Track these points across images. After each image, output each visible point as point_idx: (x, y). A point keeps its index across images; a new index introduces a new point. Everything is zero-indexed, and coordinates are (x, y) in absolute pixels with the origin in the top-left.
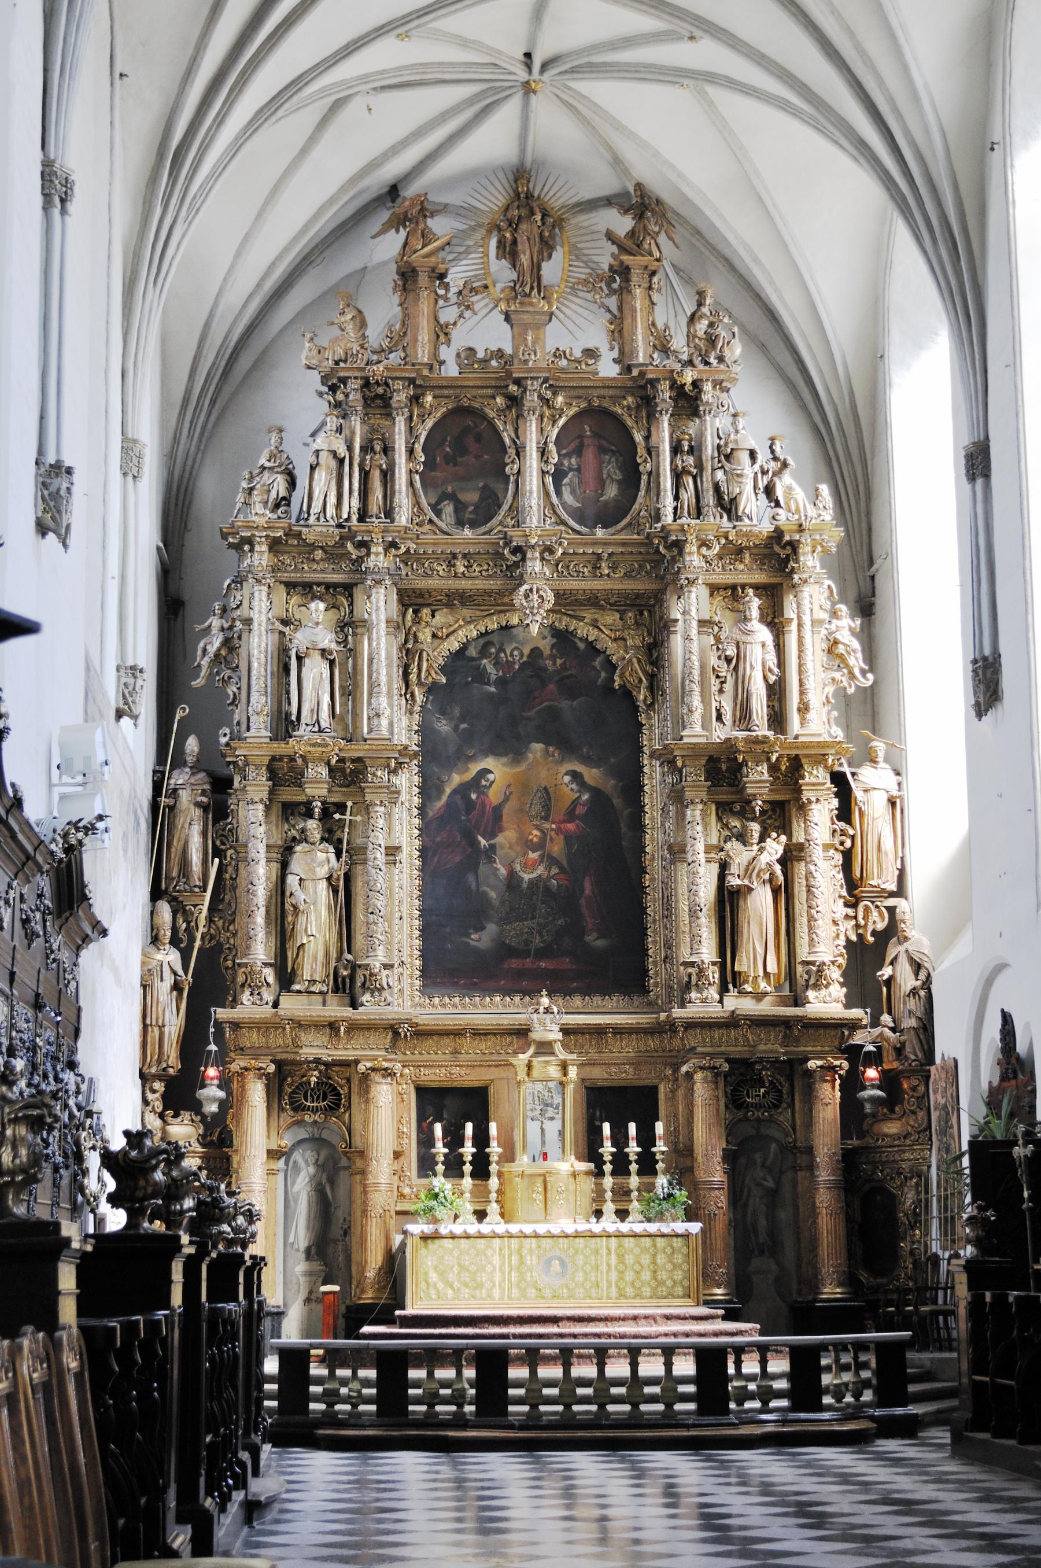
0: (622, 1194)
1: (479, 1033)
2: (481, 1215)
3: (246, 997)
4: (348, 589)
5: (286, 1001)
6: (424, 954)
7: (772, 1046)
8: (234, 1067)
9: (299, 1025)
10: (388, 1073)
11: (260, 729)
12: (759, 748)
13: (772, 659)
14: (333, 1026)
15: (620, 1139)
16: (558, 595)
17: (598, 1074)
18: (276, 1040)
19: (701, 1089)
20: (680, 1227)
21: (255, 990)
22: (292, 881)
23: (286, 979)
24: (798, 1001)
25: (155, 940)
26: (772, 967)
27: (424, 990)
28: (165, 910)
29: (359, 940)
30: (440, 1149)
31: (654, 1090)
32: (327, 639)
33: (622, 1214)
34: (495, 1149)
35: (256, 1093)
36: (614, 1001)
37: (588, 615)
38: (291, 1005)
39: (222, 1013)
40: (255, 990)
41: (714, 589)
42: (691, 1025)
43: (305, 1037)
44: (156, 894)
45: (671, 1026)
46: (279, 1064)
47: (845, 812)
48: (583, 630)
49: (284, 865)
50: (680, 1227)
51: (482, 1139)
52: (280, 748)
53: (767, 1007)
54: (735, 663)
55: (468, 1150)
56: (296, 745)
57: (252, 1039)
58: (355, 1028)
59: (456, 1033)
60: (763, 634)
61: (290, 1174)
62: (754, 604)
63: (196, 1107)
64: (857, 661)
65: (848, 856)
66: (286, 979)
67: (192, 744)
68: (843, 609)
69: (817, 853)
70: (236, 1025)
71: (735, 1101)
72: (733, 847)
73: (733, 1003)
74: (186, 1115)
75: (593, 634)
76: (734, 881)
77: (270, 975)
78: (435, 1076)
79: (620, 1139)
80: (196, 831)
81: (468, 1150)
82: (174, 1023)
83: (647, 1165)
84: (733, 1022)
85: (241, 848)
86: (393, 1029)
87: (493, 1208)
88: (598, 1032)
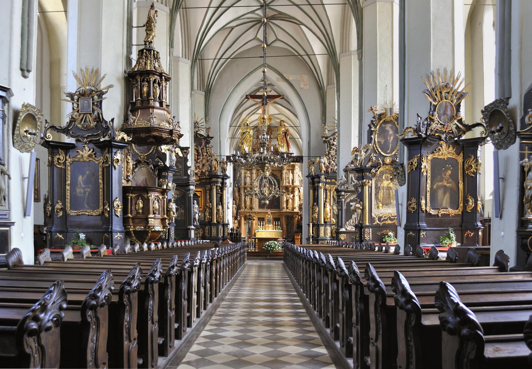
0: (276, 228)
1: (263, 213)
2: (263, 229)
3: (242, 209)
4: (251, 170)
5: (245, 210)
6: (259, 205)
7: (290, 214)
8: (241, 216)
9: (247, 212)
10: (255, 217)
11: (243, 184)
12: (290, 186)
13: (292, 177)
14: (250, 212)
15: (276, 223)
16: (272, 170)
17: (275, 217)
18: (244, 213)
19: (284, 218)
20: (280, 231)
21: (243, 209)
22: (246, 198)
23: (246, 207)
24: (293, 210)
25: (233, 204)
26: (291, 207)
27: (259, 208)
28: (234, 202)
29: (252, 204)
30: (259, 224)
31: (280, 218)
32: (249, 175)
33: (276, 230)
34: (264, 224)
35: (243, 218)
36: (277, 210)
37: (275, 171)
38: (246, 210)
39: (239, 211)
40: (243, 209)
41: (287, 169)
42: (283, 212)
43: (247, 213)
44: (233, 200)
45: (281, 213)
46: (245, 216)
47: (299, 192)
48: (275, 173)
49: (245, 197)
50: (280, 231)
51: (263, 223)
52: (245, 186)
53: (290, 211)
54: (288, 178)
55: (262, 224)
56: (246, 186)
57: (242, 213)
58: (252, 212)
59: (261, 213)
60: (291, 175)
61: (246, 225)
62: (291, 171)
63: (237, 219)
64: (301, 177)
65: (299, 196)
66: (246, 207)
67: (237, 185)
68: (300, 171)
69: (296, 196)
70: (241, 212)
71: (287, 219)
72: (287, 195)
73: (287, 210)
74: (236, 220)
75: (275, 173)
76: (288, 199)
77: (244, 207)
78: (259, 217)
79: (276, 223)
80: (237, 194)
81: (262, 224)
82: (235, 212)
83: (278, 225)
84: (286, 212)
85: (241, 195)
86: (255, 212)
87: (264, 229)
88: (275, 213)
